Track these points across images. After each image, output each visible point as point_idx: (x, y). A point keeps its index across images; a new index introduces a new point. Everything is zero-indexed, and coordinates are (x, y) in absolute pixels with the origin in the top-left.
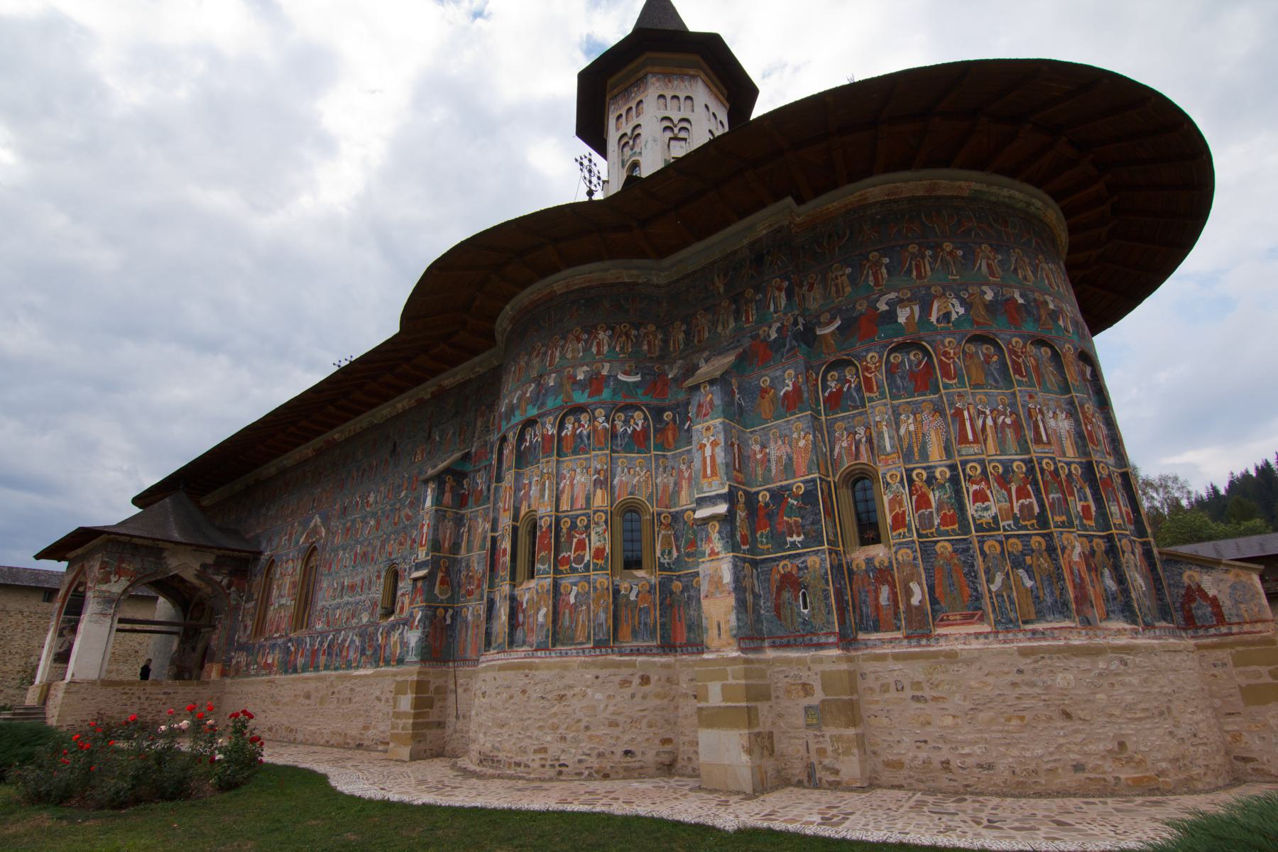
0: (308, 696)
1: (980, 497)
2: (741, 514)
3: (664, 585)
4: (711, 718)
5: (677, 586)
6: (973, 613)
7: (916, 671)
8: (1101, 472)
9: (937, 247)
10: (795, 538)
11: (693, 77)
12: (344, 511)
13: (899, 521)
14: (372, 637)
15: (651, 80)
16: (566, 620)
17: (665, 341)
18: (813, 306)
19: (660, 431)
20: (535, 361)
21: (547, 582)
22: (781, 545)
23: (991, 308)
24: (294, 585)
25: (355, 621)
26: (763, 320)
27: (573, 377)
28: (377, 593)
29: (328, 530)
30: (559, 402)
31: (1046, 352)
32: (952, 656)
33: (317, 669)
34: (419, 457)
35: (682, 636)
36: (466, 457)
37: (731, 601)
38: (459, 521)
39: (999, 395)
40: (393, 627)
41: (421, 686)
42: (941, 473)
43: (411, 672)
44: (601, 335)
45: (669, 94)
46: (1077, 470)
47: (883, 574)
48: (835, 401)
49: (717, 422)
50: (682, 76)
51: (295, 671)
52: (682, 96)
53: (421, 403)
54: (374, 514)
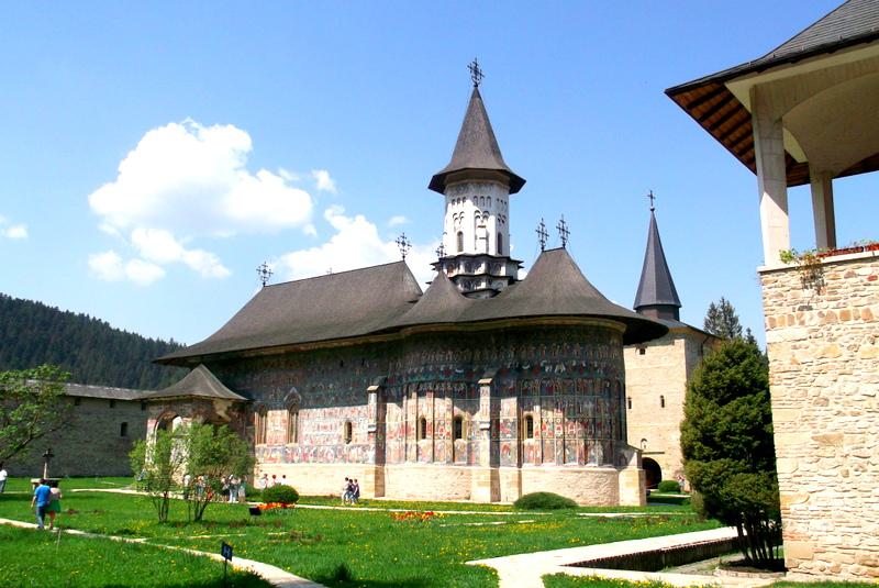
0: (306, 474)
1: (559, 429)
2: (494, 427)
3: (469, 446)
4: (480, 484)
5: (473, 445)
6: (552, 460)
7: (534, 474)
8: (598, 421)
9: (561, 345)
10: (509, 435)
11: (492, 184)
12: (313, 390)
13: (537, 434)
14: (340, 451)
15: (471, 187)
16: (436, 455)
17: (473, 355)
18: (523, 356)
19: (470, 391)
20: (423, 357)
21: (431, 442)
22: (505, 437)
23: (574, 368)
24: (284, 421)
25: (328, 443)
26: (506, 359)
27: (439, 369)
28: (342, 431)
29: (303, 397)
30: (434, 377)
31: (591, 381)
32: (544, 471)
33: (308, 462)
34: (358, 373)
35: (474, 461)
36: (386, 379)
37: (489, 453)
38: (385, 408)
39: (571, 397)
40: (352, 447)
41: (376, 472)
42: (551, 420)
43: (372, 466)
44: (450, 353)
45: (479, 195)
46: (591, 420)
47: (531, 448)
48: (526, 392)
49: (488, 398)
50: (485, 184)
51: (293, 462)
52: (486, 196)
53: (356, 346)
54: (334, 395)
